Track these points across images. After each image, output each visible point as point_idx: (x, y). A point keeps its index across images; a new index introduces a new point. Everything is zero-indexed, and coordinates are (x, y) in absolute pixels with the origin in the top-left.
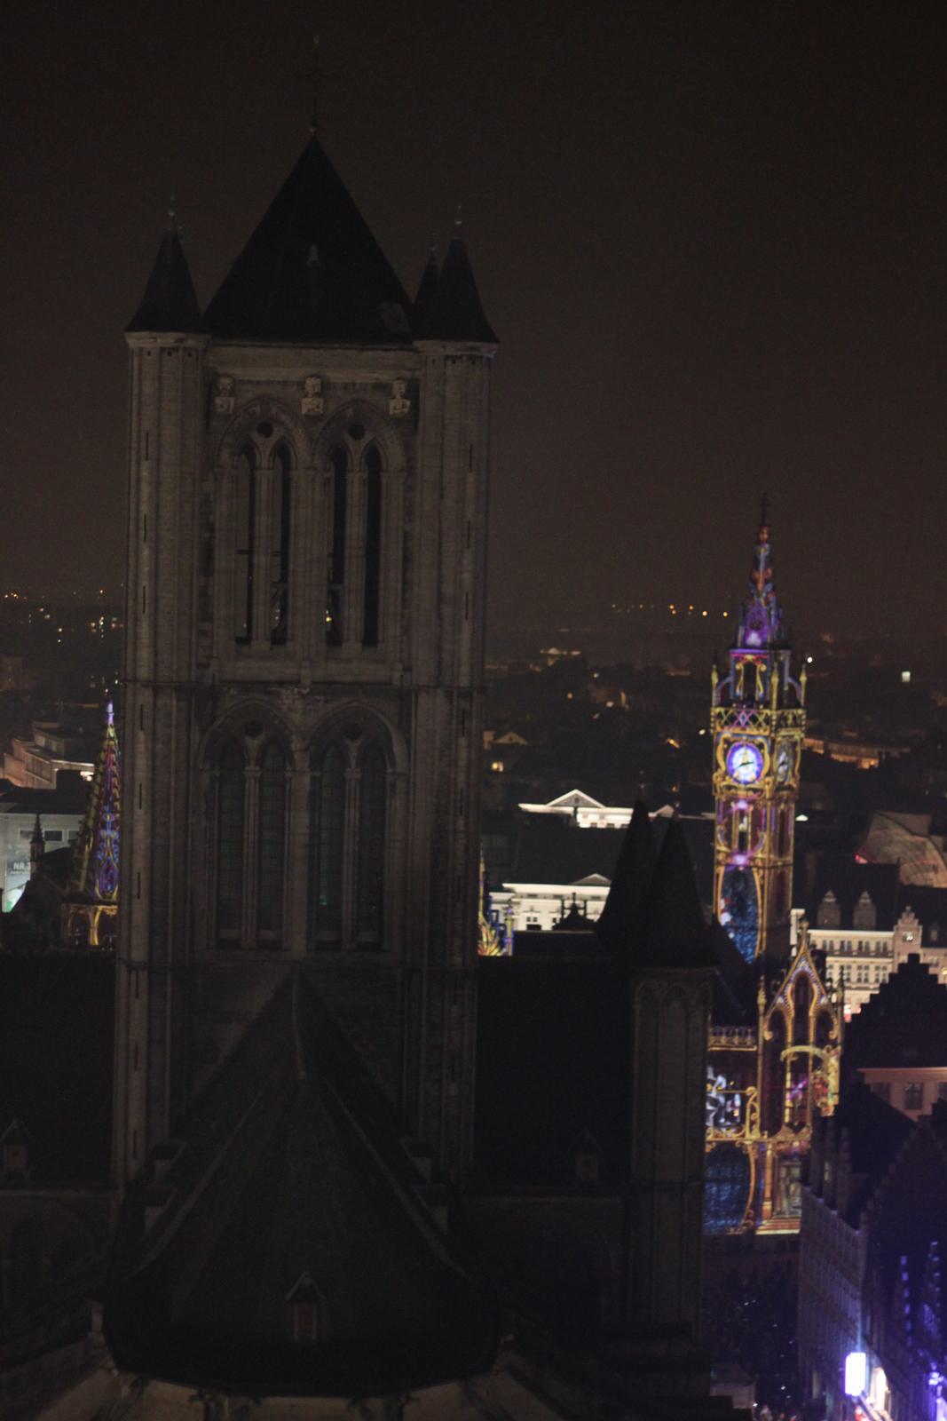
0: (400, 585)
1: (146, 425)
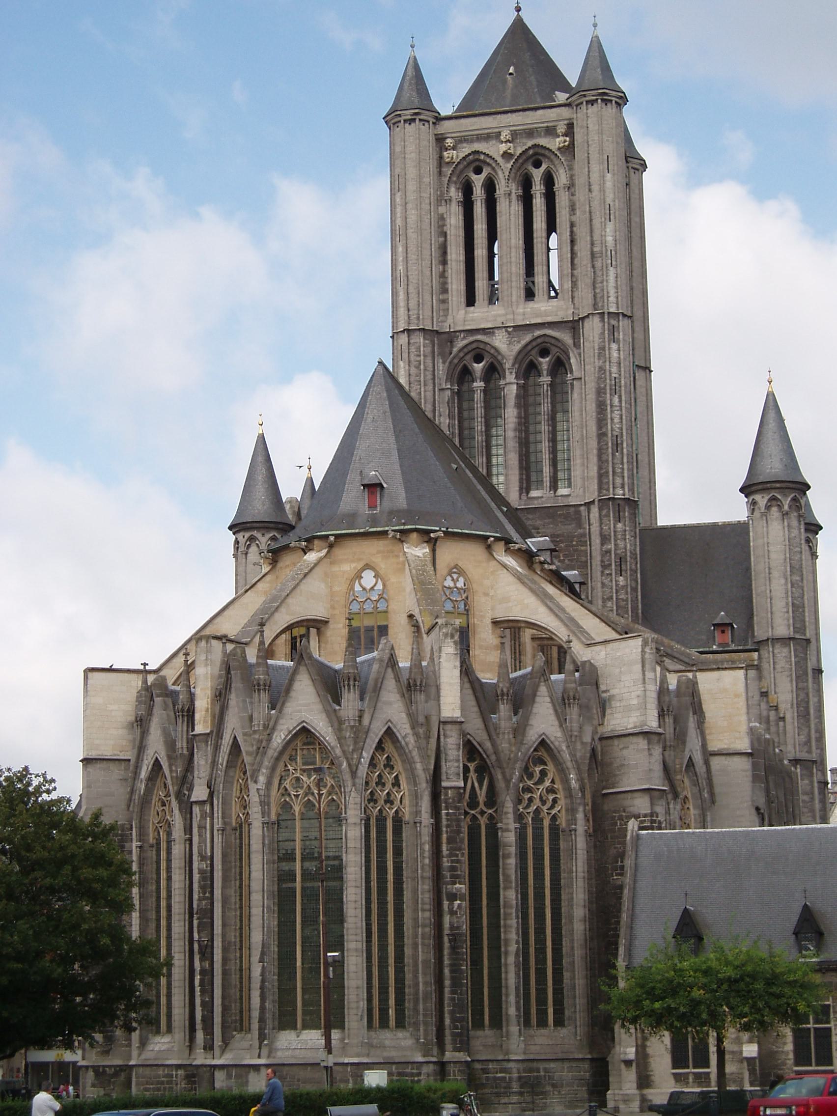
0: (569, 255)
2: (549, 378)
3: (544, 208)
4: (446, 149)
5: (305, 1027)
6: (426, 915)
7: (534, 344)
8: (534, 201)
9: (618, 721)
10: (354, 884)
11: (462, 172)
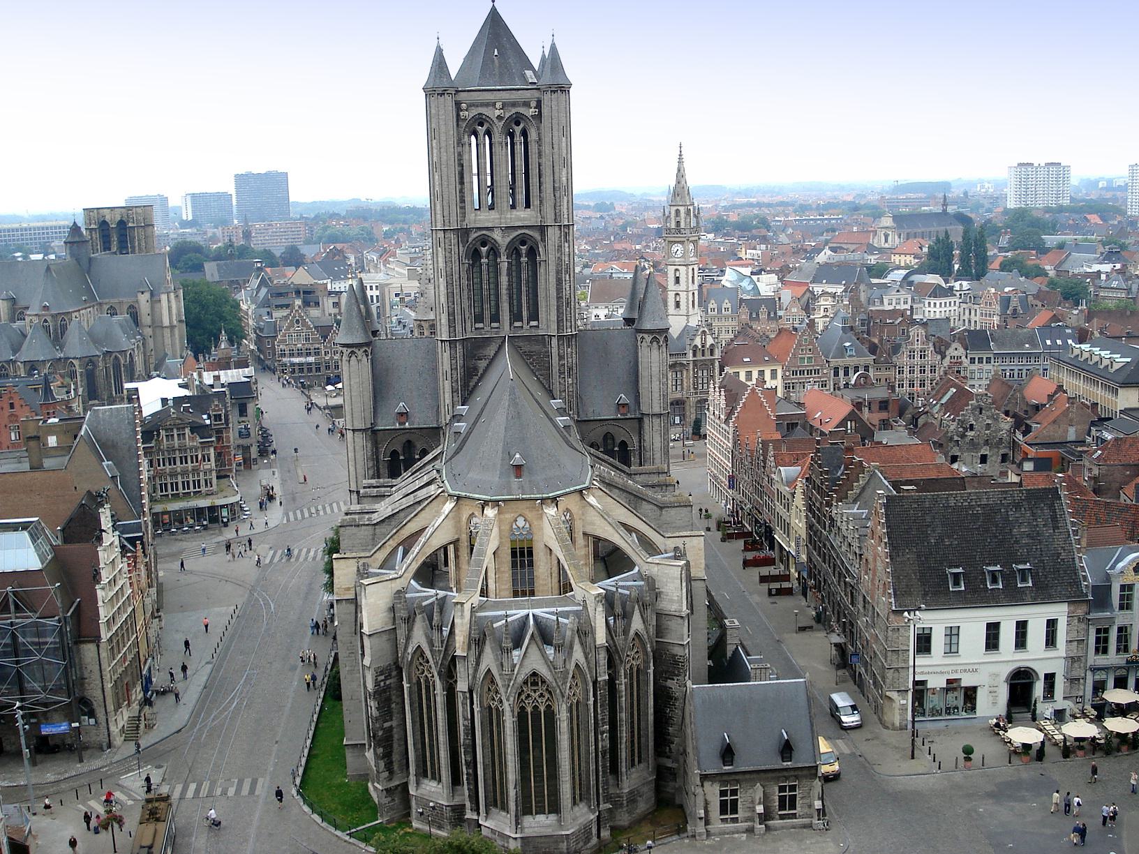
1: (433, 126)
2: (526, 259)
4: (462, 111)
5: (536, 814)
11: (472, 125)
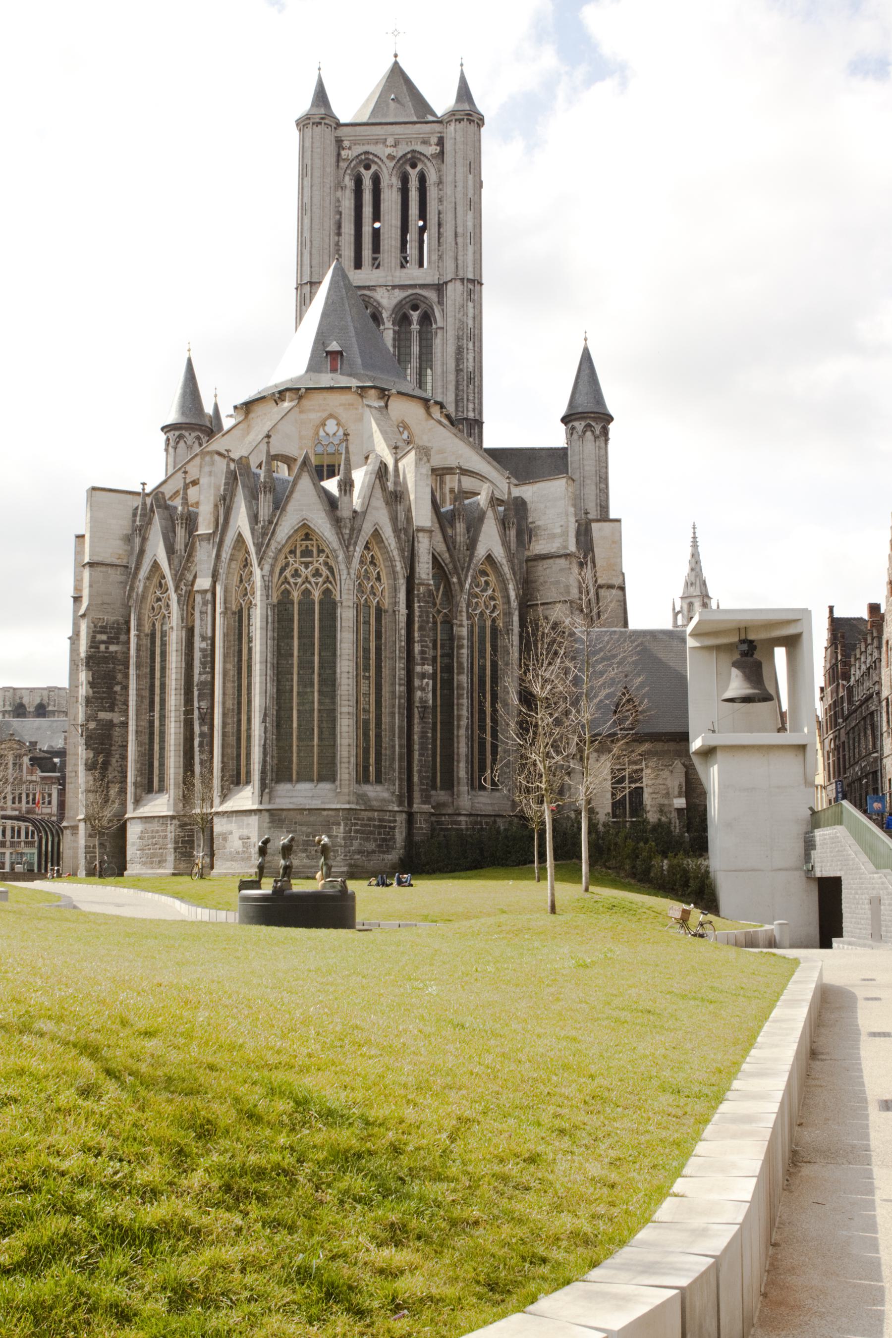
2: (418, 327)
3: (417, 199)
4: (343, 149)
5: (299, 780)
6: (400, 689)
7: (408, 300)
8: (410, 193)
9: (542, 547)
10: (347, 657)
